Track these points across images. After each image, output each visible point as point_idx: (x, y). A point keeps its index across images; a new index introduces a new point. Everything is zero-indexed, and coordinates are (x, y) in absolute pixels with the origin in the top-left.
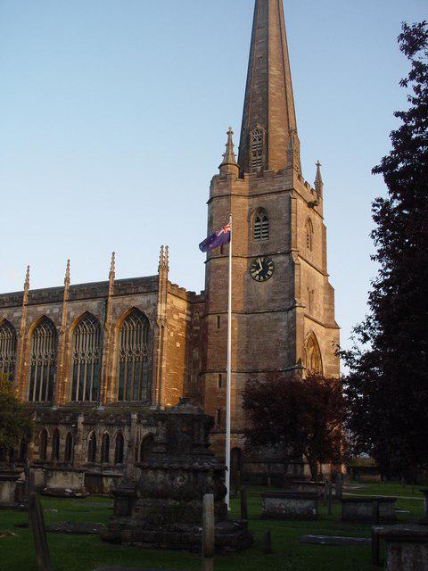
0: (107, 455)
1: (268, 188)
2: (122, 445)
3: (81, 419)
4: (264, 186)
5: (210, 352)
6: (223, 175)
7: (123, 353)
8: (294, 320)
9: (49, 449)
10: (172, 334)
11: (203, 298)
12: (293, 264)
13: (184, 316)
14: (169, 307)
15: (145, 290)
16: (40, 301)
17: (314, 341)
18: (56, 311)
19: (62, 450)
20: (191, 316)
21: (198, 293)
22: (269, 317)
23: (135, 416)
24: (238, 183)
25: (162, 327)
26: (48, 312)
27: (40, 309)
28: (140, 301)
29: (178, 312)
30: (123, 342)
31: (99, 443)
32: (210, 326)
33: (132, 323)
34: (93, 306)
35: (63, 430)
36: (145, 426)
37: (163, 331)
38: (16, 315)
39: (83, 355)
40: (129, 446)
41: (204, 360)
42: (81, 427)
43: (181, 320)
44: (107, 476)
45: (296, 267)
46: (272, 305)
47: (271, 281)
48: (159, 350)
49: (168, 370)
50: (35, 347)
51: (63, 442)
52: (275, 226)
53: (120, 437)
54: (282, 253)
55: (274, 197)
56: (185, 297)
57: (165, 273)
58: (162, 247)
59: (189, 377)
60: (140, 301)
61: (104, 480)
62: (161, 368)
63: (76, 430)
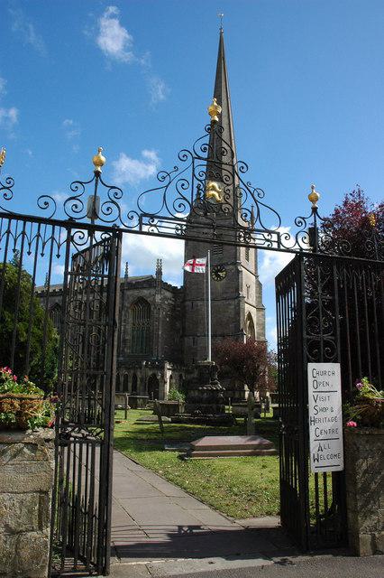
2: (136, 381)
12: (239, 272)
17: (250, 317)
20: (175, 301)
21: (179, 288)
31: (122, 379)
41: (184, 328)
53: (135, 377)
60: (145, 292)
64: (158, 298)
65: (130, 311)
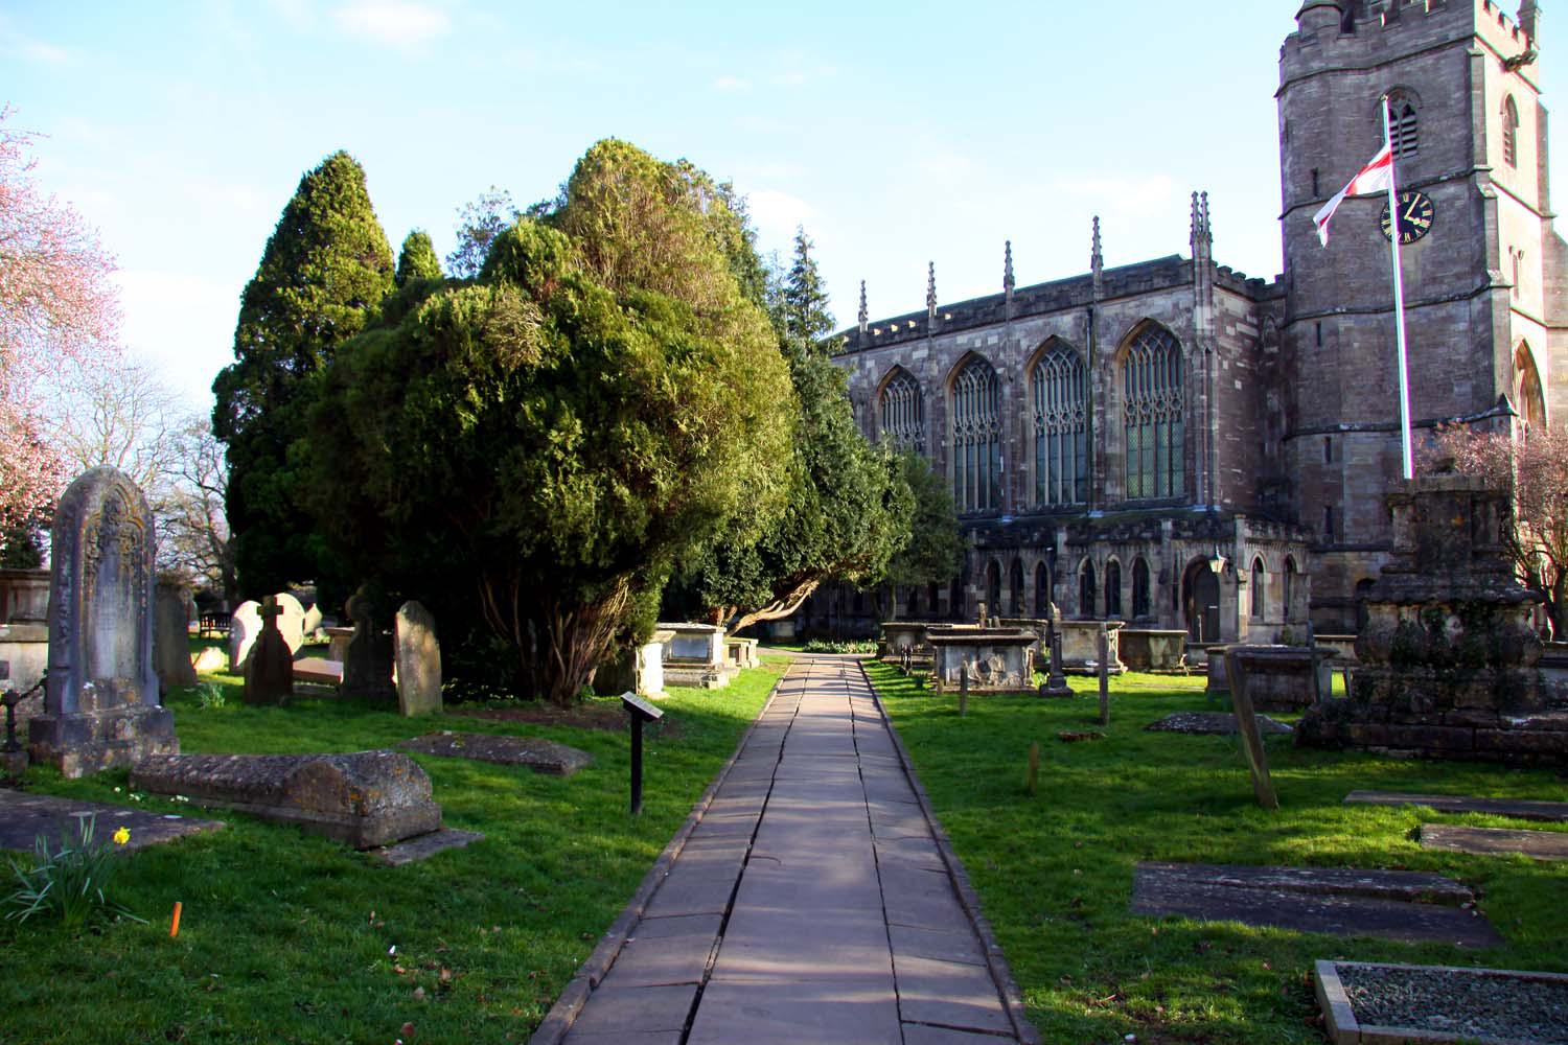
0: (1117, 600)
1: (1409, 44)
3: (1062, 537)
4: (1401, 40)
5: (1303, 396)
6: (1307, 32)
7: (1130, 407)
8: (1486, 316)
9: (1005, 595)
10: (1226, 365)
11: (1281, 289)
12: (1480, 201)
13: (1241, 327)
14: (1216, 312)
15: (1167, 284)
16: (961, 326)
17: (1526, 359)
18: (993, 340)
19: (1031, 594)
20: (1259, 327)
21: (1270, 280)
22: (1427, 315)
23: (1168, 525)
24: (1343, 42)
25: (1208, 352)
26: (978, 344)
27: (962, 339)
28: (1158, 305)
29: (1233, 321)
30: (1130, 388)
31: (1100, 579)
32: (1300, 344)
33: (1144, 349)
34: (1066, 323)
35: (1031, 560)
36: (1190, 541)
37: (1209, 360)
38: (916, 355)
39: (1052, 417)
40: (1162, 581)
41: (1293, 411)
42: (1062, 550)
43: (1241, 336)
44: (1156, 636)
45: (1487, 204)
46: (1431, 291)
47: (1428, 240)
48: (1204, 397)
49: (1222, 435)
50: (958, 412)
51: (1030, 580)
52: (1430, 123)
53: (1141, 569)
54: (1451, 180)
55: (1428, 60)
56: (1243, 290)
57: (1205, 246)
58: (1195, 195)
59: (1262, 446)
60: (1158, 305)
61: (1152, 642)
62: (1210, 431)
63: (1054, 556)
64: (1203, 318)
65: (1115, 366)
